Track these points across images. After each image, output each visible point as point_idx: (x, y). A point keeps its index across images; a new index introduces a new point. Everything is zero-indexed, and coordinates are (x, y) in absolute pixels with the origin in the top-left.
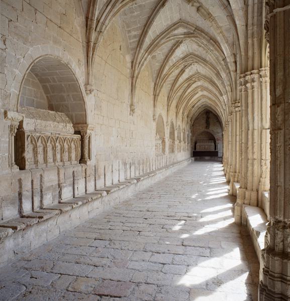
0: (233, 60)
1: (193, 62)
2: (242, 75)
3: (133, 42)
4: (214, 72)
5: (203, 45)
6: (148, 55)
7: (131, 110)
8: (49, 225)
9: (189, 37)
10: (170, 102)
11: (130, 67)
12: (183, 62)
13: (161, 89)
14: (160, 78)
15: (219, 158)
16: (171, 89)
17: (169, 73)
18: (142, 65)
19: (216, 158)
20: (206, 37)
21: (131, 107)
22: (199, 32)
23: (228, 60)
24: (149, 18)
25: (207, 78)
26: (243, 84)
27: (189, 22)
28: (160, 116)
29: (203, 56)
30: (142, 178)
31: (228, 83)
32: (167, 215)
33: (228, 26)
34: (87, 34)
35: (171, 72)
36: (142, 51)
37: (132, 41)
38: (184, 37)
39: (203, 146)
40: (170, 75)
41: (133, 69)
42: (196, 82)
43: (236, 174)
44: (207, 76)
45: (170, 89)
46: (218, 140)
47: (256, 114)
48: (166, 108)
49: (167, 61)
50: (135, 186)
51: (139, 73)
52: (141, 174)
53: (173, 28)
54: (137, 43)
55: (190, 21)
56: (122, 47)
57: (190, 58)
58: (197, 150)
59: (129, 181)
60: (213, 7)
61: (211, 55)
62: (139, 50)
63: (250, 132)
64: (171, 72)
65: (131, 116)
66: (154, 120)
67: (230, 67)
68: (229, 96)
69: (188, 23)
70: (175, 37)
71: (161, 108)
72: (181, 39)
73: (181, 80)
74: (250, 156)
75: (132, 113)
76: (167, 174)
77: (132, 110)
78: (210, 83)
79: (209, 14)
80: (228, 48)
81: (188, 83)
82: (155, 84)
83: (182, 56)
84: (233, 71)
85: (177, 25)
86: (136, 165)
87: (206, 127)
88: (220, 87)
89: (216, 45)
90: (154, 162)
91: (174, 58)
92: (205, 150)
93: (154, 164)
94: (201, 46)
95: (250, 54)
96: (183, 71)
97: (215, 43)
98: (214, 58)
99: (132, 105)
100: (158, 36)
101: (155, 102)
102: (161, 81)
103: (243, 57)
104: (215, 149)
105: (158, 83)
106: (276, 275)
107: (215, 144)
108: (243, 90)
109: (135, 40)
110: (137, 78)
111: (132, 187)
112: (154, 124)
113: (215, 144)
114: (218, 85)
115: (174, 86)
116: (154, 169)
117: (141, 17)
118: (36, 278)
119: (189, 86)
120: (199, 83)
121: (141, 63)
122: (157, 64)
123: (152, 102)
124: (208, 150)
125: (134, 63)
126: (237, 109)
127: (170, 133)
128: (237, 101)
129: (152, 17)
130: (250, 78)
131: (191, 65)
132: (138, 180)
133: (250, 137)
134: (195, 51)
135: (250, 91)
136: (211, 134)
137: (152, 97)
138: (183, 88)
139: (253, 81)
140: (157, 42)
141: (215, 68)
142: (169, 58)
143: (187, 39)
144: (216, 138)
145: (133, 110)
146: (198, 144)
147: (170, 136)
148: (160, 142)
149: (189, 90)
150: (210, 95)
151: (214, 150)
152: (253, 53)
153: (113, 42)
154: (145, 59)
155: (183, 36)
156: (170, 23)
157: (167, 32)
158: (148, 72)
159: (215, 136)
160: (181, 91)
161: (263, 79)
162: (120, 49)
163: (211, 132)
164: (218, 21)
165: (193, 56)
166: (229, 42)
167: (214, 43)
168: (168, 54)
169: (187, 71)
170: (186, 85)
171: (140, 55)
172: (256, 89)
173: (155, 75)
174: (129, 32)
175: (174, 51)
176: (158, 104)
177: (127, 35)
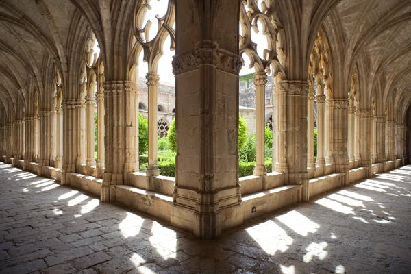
0: (65, 62)
2: (107, 82)
23: (61, 60)
31: (41, 79)
63: (115, 128)
69: (13, 7)
74: (115, 146)
95: (116, 66)
126: (69, 107)
133: (115, 132)
135: (115, 96)
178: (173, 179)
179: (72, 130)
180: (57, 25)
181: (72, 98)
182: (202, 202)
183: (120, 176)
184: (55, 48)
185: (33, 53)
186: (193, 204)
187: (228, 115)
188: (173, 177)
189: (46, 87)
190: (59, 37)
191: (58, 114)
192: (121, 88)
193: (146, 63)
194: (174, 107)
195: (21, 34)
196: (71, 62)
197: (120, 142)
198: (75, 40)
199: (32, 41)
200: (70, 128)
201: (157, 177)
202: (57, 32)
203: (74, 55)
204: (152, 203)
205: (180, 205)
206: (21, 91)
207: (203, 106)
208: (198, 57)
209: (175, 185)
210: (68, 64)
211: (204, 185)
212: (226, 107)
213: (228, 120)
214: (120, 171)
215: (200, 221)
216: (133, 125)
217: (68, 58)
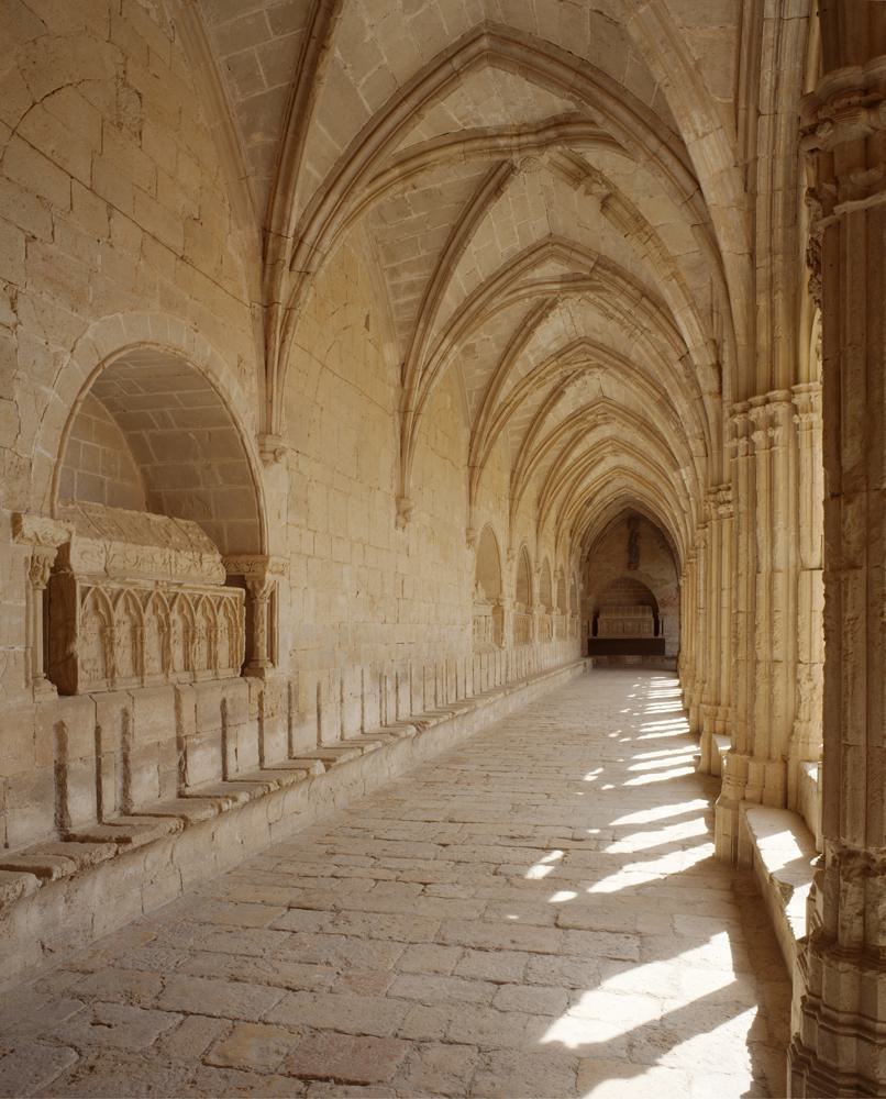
0: (710, 360)
1: (588, 367)
2: (739, 407)
3: (407, 304)
4: (653, 397)
5: (618, 315)
6: (452, 345)
7: (398, 513)
8: (148, 865)
9: (577, 290)
10: (519, 487)
11: (397, 381)
12: (559, 366)
13: (490, 447)
14: (487, 416)
15: (667, 658)
16: (523, 449)
18: (434, 375)
19: (658, 659)
21: (398, 503)
22: (608, 273)
23: (696, 361)
24: (455, 229)
26: (740, 432)
27: (575, 243)
28: (489, 531)
30: (433, 722)
31: (696, 430)
32: (510, 834)
33: (696, 256)
34: (267, 278)
35: (519, 396)
36: (434, 332)
37: (402, 300)
38: (563, 290)
39: (620, 624)
40: (517, 404)
42: (596, 426)
43: (721, 710)
44: (632, 407)
45: (517, 447)
46: (665, 605)
47: (780, 523)
48: (506, 504)
49: (511, 363)
50: (413, 744)
51: (422, 400)
52: (431, 707)
53: (528, 261)
54: (416, 307)
55: (579, 240)
56: (371, 320)
57: (578, 353)
58: (600, 636)
59: (392, 730)
60: (651, 197)
61: (643, 343)
62: (425, 330)
63: (762, 580)
64: (519, 396)
65: (400, 531)
66: (470, 541)
67: (701, 381)
68: (699, 471)
69: (572, 247)
70: (533, 289)
71: (491, 505)
72: (551, 297)
73: (553, 419)
74: (763, 652)
75: (402, 520)
76: (511, 710)
77: (404, 514)
78: (639, 429)
79: (638, 218)
80: (694, 322)
81: (574, 430)
82: (473, 433)
83: (555, 347)
84: (710, 394)
86: (415, 681)
87: (630, 563)
88: (670, 444)
89: (658, 315)
90: (469, 670)
91: (532, 352)
92: (625, 637)
93: (469, 678)
94: (612, 317)
95: (763, 340)
96: (557, 394)
97: (658, 309)
98: (655, 353)
99: (401, 497)
101: (474, 487)
102: (490, 423)
103: (740, 349)
104: (656, 633)
105: (483, 427)
106: (842, 1018)
108: (741, 452)
109: (412, 297)
110: (417, 414)
111: (402, 749)
112: (469, 557)
114: (666, 436)
115: (532, 439)
116: (470, 695)
117: (429, 227)
118: (109, 1026)
119: (576, 440)
120: (606, 431)
121: (431, 368)
122: (478, 372)
123: (464, 488)
124: (637, 636)
126: (723, 510)
127: (519, 582)
128: (725, 486)
129: (464, 226)
130: (761, 415)
131: (583, 373)
132: (421, 726)
133: (762, 593)
134: (595, 330)
135: (762, 455)
136: (645, 587)
137: (464, 472)
138: (559, 446)
139: (772, 423)
140: (480, 301)
141: (656, 385)
142: (516, 352)
143: (572, 294)
144: (658, 599)
145: (404, 513)
146: (602, 617)
147: (518, 591)
148: (488, 610)
149: (577, 453)
150: (640, 468)
151: (652, 636)
152: (773, 338)
153: (345, 305)
154: (443, 358)
155: (558, 286)
156: (518, 245)
157: (509, 275)
158: (452, 396)
159: (653, 592)
160: (553, 453)
161: (804, 416)
162: (367, 326)
163: (644, 581)
164: (664, 240)
165: (588, 347)
167: (654, 309)
168: (512, 342)
169: (570, 392)
170: (568, 435)
171: (427, 345)
172: (780, 450)
173: (472, 406)
174: (394, 272)
175: (530, 332)
176: (484, 494)
177: (388, 282)
180: (673, 251)
183: (774, 772)
190: (683, 286)
192: (781, 418)
197: (779, 634)
202: (675, 275)
206: (680, 474)
214: (776, 754)
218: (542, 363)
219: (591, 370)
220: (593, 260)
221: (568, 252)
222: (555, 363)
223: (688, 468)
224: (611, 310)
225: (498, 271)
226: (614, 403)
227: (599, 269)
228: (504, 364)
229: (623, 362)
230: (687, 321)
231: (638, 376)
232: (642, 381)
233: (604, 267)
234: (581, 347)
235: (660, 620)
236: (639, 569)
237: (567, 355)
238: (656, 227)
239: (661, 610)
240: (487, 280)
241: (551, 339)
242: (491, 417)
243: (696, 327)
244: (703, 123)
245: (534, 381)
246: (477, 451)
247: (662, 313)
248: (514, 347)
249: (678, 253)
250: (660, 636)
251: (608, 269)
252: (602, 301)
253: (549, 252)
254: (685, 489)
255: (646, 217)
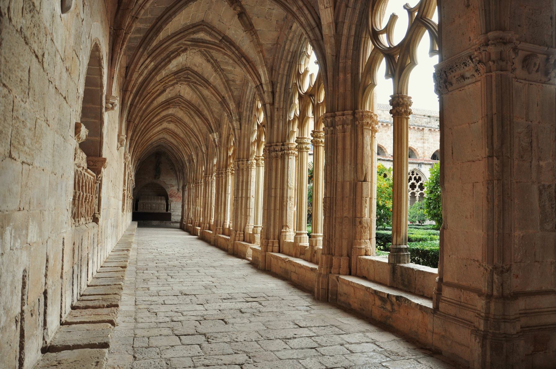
0: (270, 90)
3: (135, 38)
4: (218, 99)
5: (212, 61)
6: (151, 62)
9: (197, 46)
12: (176, 78)
17: (153, 91)
20: (236, 52)
22: (228, 44)
23: (265, 89)
24: (168, 9)
25: (193, 105)
29: (206, 76)
31: (237, 117)
33: (270, 46)
34: (119, 16)
39: (149, 205)
41: (128, 78)
44: (193, 102)
47: (348, 161)
54: (139, 40)
55: (217, 26)
57: (185, 74)
58: (140, 210)
60: (258, 17)
69: (213, 28)
79: (251, 24)
80: (266, 72)
83: (175, 69)
85: (198, 27)
89: (248, 66)
92: (152, 211)
97: (248, 63)
98: (224, 80)
100: (168, 36)
104: (167, 210)
107: (167, 202)
109: (138, 35)
113: (167, 202)
117: (156, 5)
124: (157, 211)
125: (130, 71)
126: (273, 154)
130: (342, 119)
134: (195, 65)
135: (340, 135)
140: (167, 44)
144: (169, 193)
146: (141, 202)
151: (165, 211)
156: (188, 22)
157: (183, 34)
164: (259, 36)
166: (268, 66)
172: (348, 134)
178: (435, 271)
179: (276, 189)
180: (262, 41)
181: (277, 142)
182: (488, 313)
184: (258, 73)
185: (231, 83)
186: (469, 315)
187: (539, 159)
188: (435, 266)
189: (243, 128)
190: (263, 56)
191: (258, 165)
193: (391, 80)
194: (437, 147)
195: (218, 60)
196: (278, 90)
198: (284, 58)
199: (230, 68)
200: (273, 186)
201: (406, 265)
203: (282, 78)
204: (396, 307)
205: (446, 316)
206: (213, 136)
207: (491, 144)
208: (480, 62)
209: (437, 278)
210: (273, 93)
211: (491, 283)
212: (534, 144)
213: (539, 167)
215: (483, 346)
216: (369, 179)
217: (273, 84)
218: (167, 76)
219: (181, 82)
220: (221, 36)
221: (210, 31)
222: (173, 77)
223: (217, 133)
224: (209, 58)
225: (177, 32)
226: (184, 99)
227: (223, 41)
228: (153, 74)
229: (205, 82)
230: (264, 72)
231: (211, 89)
232: (214, 92)
233: (226, 41)
234: (187, 71)
235: (169, 203)
236: (160, 179)
237: (180, 74)
238: (257, 30)
239: (170, 199)
240: (172, 34)
241: (175, 65)
242: (142, 98)
243: (267, 75)
244: (327, 3)
245: (163, 84)
246: (133, 114)
247: (250, 66)
248: (160, 66)
249: (263, 43)
250: (169, 212)
251: (228, 42)
252: (206, 53)
253: (201, 28)
254: (215, 143)
255: (254, 25)
